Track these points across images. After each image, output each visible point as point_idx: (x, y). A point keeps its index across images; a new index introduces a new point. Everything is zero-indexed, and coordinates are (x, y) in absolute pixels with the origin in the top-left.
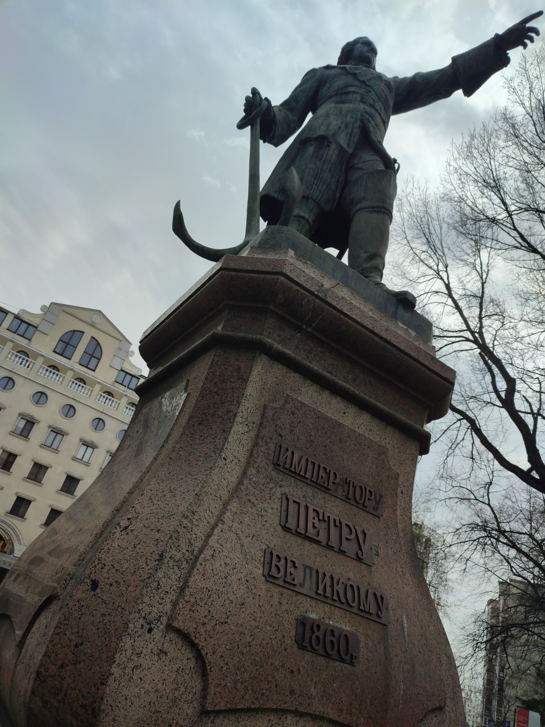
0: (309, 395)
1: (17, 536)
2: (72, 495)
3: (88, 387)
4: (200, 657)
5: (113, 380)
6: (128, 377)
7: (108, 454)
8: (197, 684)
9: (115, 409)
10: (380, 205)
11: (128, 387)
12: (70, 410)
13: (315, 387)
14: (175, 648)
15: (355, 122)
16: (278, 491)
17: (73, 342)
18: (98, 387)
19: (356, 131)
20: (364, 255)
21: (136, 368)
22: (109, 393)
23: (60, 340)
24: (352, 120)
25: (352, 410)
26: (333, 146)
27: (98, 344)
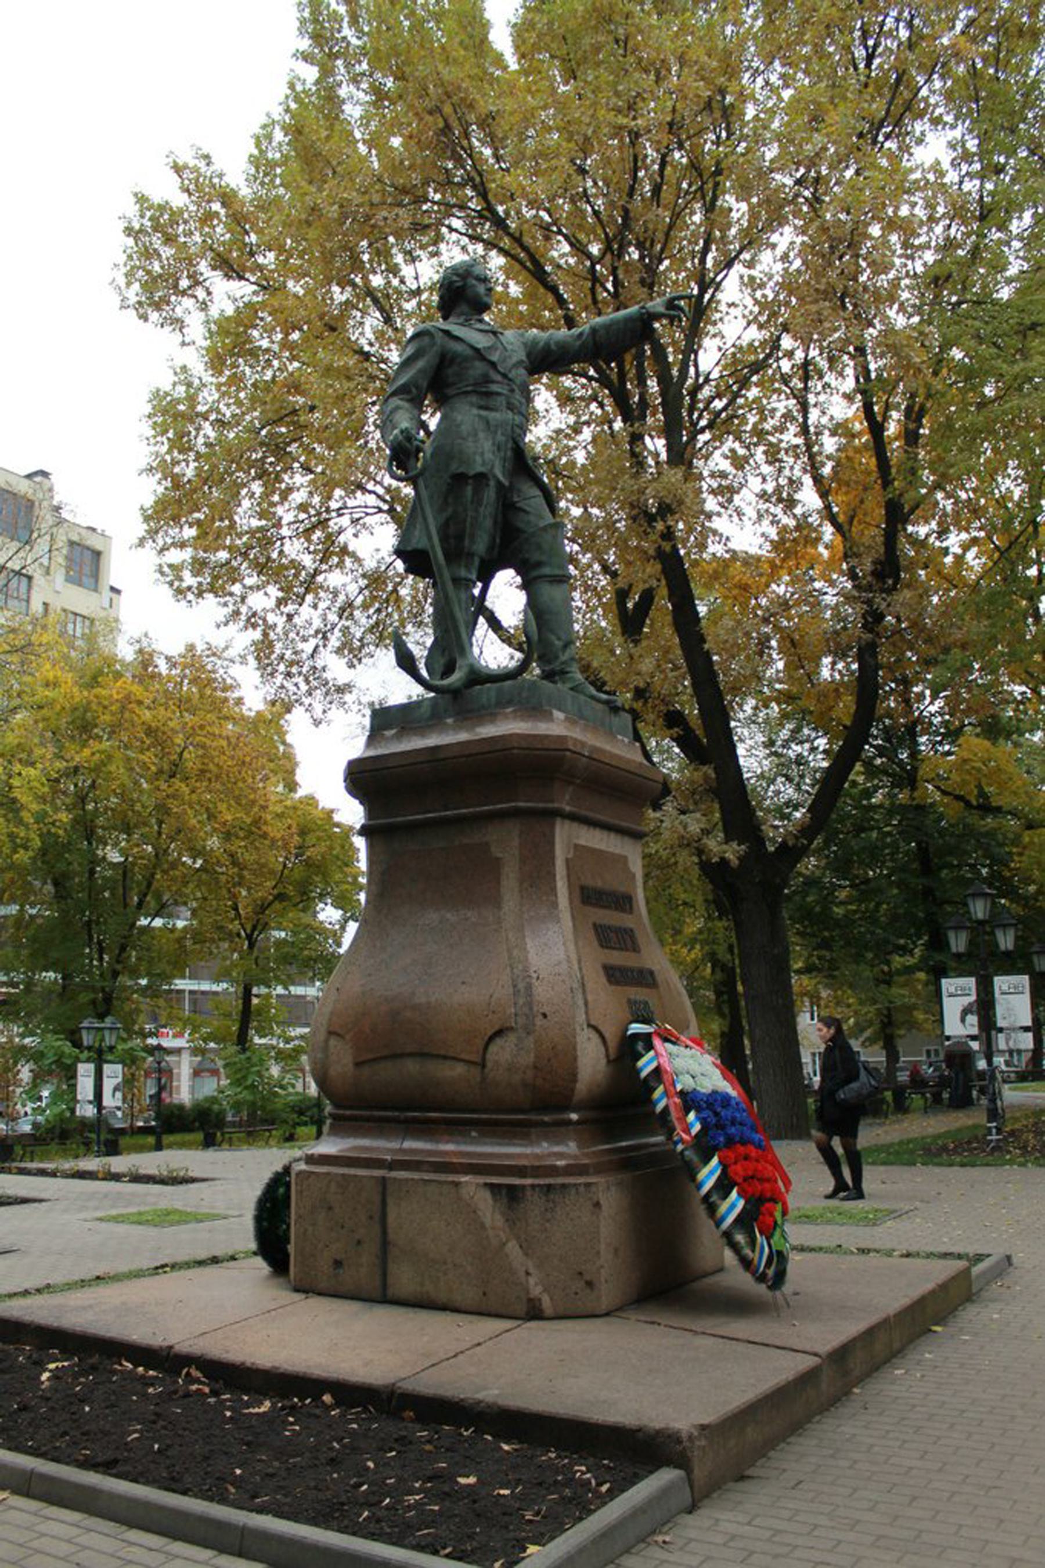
19: (509, 453)
20: (558, 644)
26: (492, 483)
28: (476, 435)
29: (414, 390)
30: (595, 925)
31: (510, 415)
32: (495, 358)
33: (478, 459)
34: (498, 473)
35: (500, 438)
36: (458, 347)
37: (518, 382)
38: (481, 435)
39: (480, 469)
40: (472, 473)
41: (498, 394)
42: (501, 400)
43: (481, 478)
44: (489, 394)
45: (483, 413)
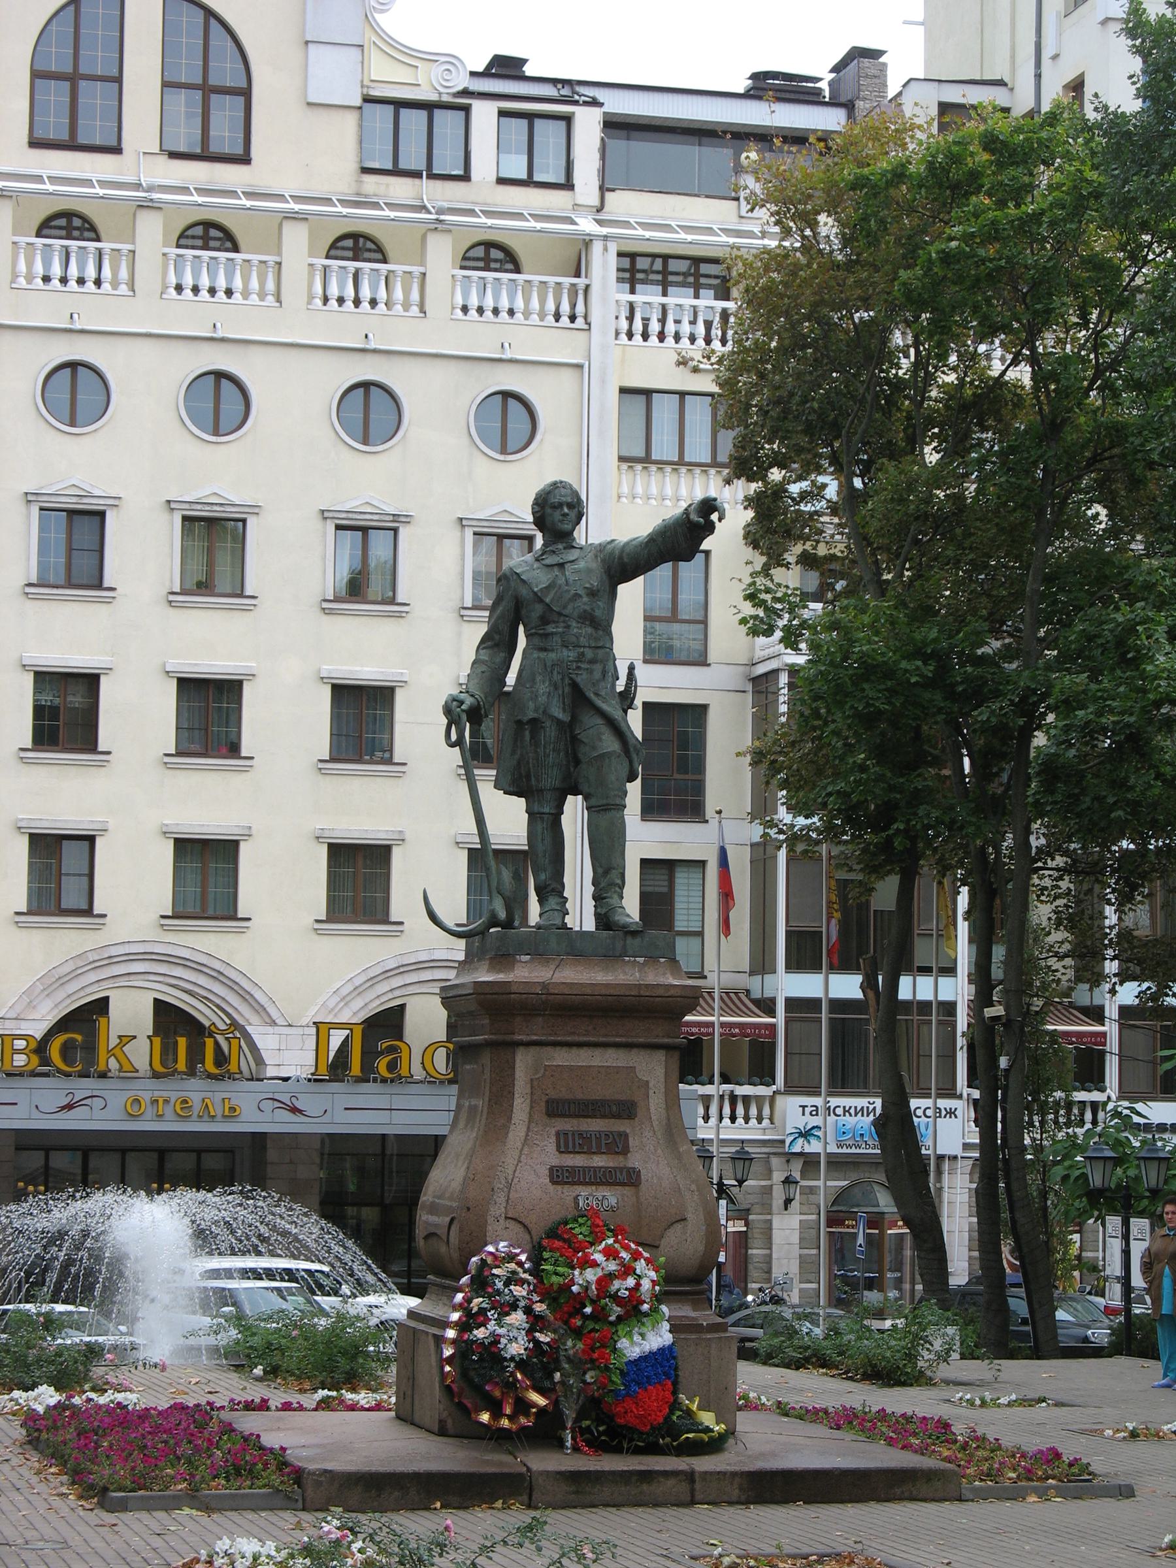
0: (561, 1058)
1: (246, 996)
2: (389, 761)
3: (255, 258)
4: (525, 1226)
5: (350, 165)
6: (414, 121)
7: (469, 533)
8: (527, 1237)
9: (415, 310)
10: (605, 802)
11: (432, 176)
12: (220, 401)
13: (565, 1049)
14: (512, 1225)
15: (562, 679)
16: (553, 1131)
17: (95, 60)
18: (296, 240)
19: (567, 690)
21: (430, 59)
22: (357, 246)
23: (37, 75)
24: (560, 677)
25: (597, 1052)
26: (548, 724)
27: (210, 13)
28: (533, 681)
29: (497, 637)
30: (558, 1134)
31: (565, 652)
32: (547, 600)
33: (531, 705)
34: (558, 713)
35: (556, 677)
36: (524, 591)
37: (576, 614)
38: (539, 678)
39: (531, 714)
40: (525, 719)
41: (552, 634)
42: (557, 639)
43: (534, 722)
44: (546, 635)
45: (543, 655)
